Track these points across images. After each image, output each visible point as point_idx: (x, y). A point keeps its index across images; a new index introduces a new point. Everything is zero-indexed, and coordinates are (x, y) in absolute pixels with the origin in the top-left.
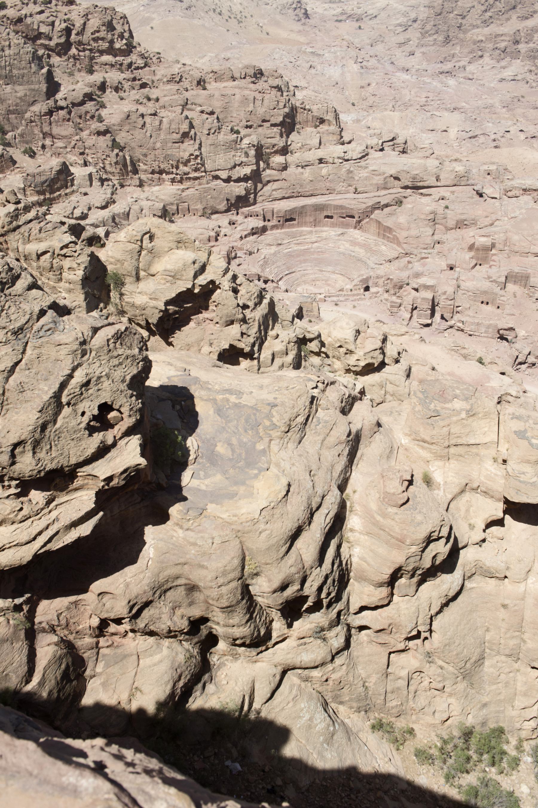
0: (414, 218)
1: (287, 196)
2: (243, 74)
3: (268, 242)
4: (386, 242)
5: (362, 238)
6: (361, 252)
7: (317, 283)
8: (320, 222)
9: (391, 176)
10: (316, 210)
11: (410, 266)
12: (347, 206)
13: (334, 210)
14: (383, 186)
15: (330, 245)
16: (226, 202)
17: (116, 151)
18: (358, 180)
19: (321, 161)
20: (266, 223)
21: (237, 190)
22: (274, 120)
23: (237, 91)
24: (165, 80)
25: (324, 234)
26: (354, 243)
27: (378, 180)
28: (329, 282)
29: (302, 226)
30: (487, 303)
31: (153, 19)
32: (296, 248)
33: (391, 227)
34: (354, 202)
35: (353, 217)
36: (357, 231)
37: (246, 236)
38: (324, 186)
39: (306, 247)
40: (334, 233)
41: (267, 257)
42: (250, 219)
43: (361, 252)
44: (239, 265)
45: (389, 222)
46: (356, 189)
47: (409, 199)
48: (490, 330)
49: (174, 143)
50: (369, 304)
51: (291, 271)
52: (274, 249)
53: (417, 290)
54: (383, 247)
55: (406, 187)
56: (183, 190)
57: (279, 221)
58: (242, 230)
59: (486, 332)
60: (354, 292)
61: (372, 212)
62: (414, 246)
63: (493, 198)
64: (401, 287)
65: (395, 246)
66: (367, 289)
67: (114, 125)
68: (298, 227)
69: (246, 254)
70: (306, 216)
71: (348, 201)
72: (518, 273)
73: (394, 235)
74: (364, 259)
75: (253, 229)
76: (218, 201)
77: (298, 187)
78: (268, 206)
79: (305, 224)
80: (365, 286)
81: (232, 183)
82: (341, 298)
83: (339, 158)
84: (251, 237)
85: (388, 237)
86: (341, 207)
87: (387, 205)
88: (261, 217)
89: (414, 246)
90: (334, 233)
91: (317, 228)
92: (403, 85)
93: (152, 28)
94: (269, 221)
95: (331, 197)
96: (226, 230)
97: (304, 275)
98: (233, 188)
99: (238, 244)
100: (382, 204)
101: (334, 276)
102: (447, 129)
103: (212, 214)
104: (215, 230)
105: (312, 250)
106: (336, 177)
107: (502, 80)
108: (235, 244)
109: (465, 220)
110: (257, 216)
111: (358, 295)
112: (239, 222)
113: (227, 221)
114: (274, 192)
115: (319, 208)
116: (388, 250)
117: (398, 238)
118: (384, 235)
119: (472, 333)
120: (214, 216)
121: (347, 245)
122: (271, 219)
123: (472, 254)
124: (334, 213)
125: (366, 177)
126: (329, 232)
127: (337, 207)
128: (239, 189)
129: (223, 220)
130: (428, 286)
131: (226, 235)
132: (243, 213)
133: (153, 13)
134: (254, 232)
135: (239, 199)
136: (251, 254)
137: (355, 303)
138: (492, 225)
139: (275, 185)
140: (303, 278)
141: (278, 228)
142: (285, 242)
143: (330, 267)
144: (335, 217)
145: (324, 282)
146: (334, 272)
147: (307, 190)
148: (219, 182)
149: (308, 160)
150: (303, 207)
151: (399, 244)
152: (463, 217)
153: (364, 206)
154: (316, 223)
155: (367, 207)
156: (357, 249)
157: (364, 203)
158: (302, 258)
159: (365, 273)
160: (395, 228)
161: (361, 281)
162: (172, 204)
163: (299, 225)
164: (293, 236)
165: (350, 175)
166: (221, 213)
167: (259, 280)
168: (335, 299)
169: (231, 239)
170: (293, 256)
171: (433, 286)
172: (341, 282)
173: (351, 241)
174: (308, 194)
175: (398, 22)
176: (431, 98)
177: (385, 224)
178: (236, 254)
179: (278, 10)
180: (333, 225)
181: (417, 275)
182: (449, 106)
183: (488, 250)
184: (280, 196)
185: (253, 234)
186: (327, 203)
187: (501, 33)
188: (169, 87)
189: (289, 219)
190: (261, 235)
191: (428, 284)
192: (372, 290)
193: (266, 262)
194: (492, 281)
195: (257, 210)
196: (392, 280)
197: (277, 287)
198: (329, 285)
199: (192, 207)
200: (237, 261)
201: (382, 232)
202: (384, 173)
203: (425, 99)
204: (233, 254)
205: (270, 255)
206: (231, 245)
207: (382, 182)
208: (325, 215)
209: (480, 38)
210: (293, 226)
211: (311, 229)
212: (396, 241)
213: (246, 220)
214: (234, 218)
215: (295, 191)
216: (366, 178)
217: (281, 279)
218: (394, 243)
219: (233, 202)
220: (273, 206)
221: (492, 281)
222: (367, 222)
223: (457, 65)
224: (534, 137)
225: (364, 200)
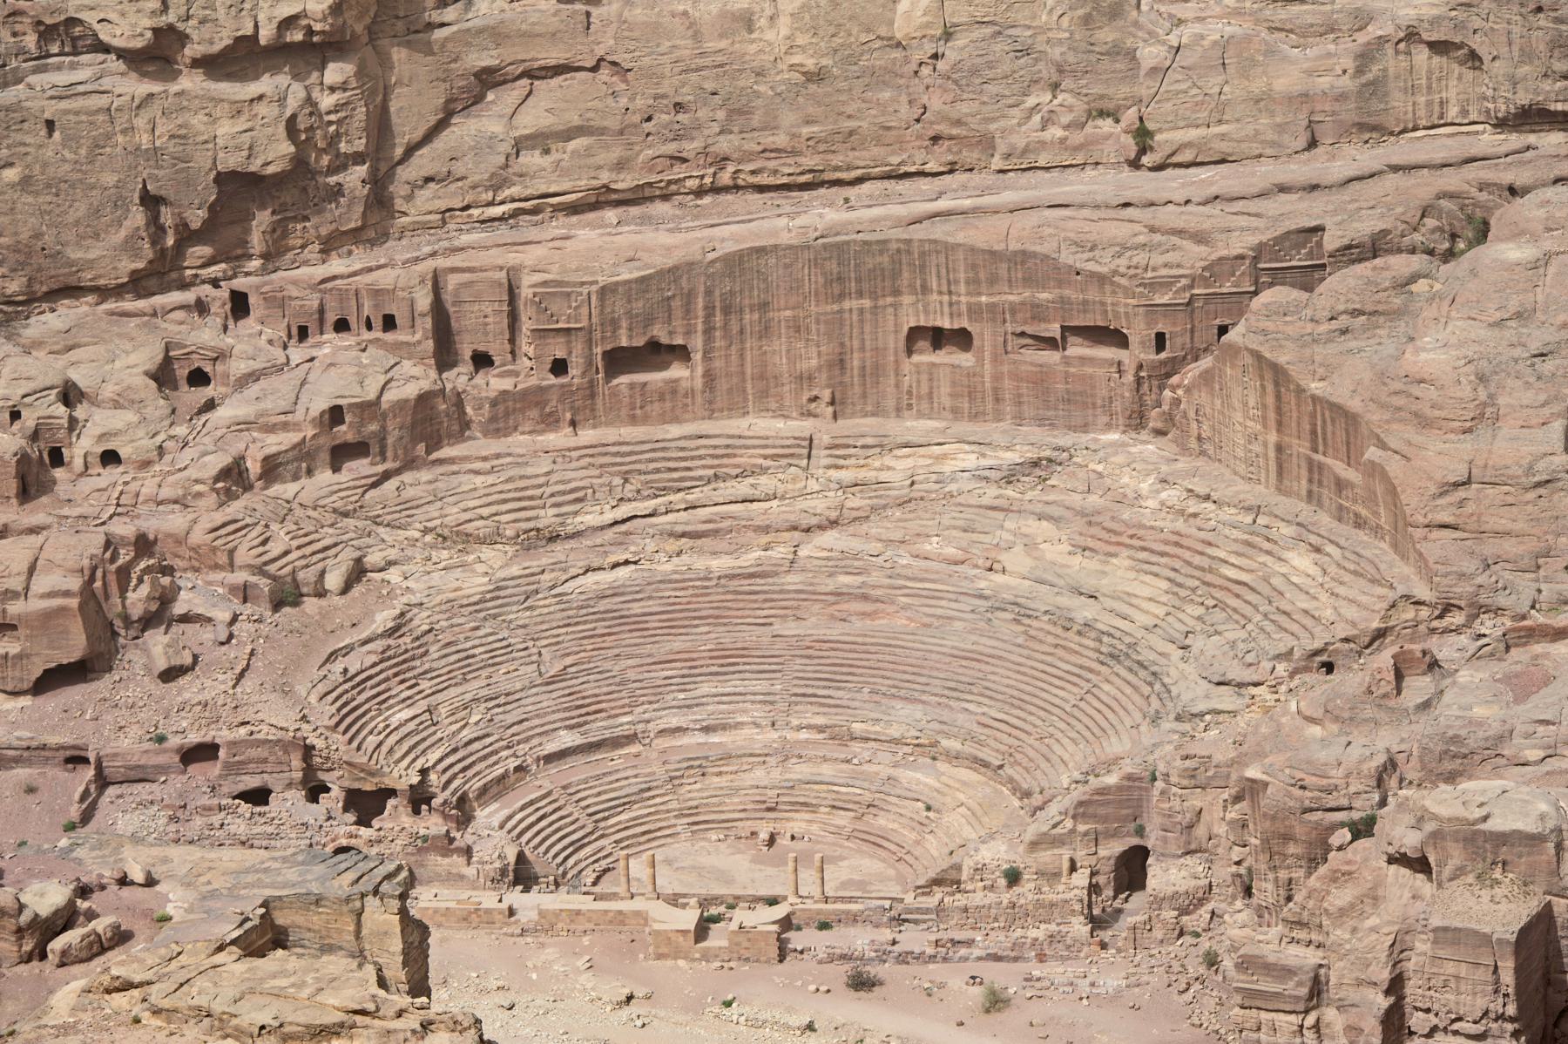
0: (1538, 338)
1: (625, 182)
3: (453, 515)
4: (1325, 520)
5: (1171, 495)
6: (1135, 594)
7: (798, 823)
8: (872, 374)
9: (1412, 36)
10: (837, 287)
11: (1418, 686)
12: (1067, 257)
13: (974, 283)
15: (932, 546)
16: (137, 217)
18: (1160, 72)
20: (459, 377)
21: (225, 129)
25: (897, 469)
26: (1105, 532)
28: (882, 822)
29: (737, 407)
32: (666, 567)
33: (1355, 405)
34: (1118, 231)
35: (1118, 339)
36: (1148, 448)
37: (272, 469)
38: (906, 112)
39: (748, 559)
40: (970, 460)
41: (421, 621)
42: (329, 344)
43: (1135, 594)
44: (170, 674)
45: (1343, 377)
46: (1143, 136)
47: (1528, 209)
50: (1111, 982)
51: (598, 729)
52: (494, 562)
53: (1421, 865)
54: (1301, 561)
55: (1531, 117)
57: (559, 367)
58: (244, 425)
60: (1026, 892)
61: (1238, 303)
62: (1509, 547)
64: (1317, 854)
65: (1379, 550)
66: (1131, 870)
68: (711, 413)
69: (245, 593)
70: (765, 331)
71: (1075, 224)
73: (1374, 470)
74: (1154, 647)
75: (335, 415)
76: (80, 210)
77: (710, 115)
78: (482, 253)
79: (765, 390)
80: (1116, 847)
81: (191, 81)
82: (914, 939)
84: (325, 477)
85: (1341, 485)
86: (1024, 265)
87: (1374, 248)
88: (421, 335)
89: (1509, 547)
90: (970, 460)
94: (482, 361)
95: (956, 194)
96: (122, 418)
97: (699, 766)
98: (198, 121)
99: (200, 522)
100: (1331, 242)
101: (919, 777)
103: (32, 300)
104: (29, 419)
105: (793, 580)
106: (999, 47)
108: (174, 521)
110: (389, 323)
112: (238, 367)
113: (148, 355)
114: (532, 159)
115: (856, 270)
116: (1322, 582)
117: (1393, 491)
120: (50, 321)
121: (1056, 551)
122: (497, 348)
124: (975, 311)
125: (1225, 44)
126: (942, 452)
127: (994, 265)
128: (245, 124)
129: (113, 354)
130: (1502, 839)
131: (110, 458)
132: (278, 302)
134: (344, 438)
135: (239, 189)
136: (286, 596)
137: (1004, 977)
139: (544, 108)
140: (693, 791)
141: (550, 422)
142: (590, 519)
143: (903, 711)
144: (984, 334)
145: (843, 819)
146: (930, 750)
147: (781, 140)
148: (86, 68)
150: (737, 263)
151: (1400, 534)
153: (1194, 256)
155: (1215, 270)
156: (1119, 575)
157: (1200, 238)
158: (705, 638)
159: (1131, 744)
160: (1375, 416)
161: (1082, 810)
163: (719, 395)
164: (669, 475)
165: (1106, 35)
166: (104, 293)
167: (315, 791)
168: (860, 939)
169: (148, 488)
170: (638, 624)
171: (1533, 840)
172: (974, 825)
173: (1089, 517)
174: (786, 170)
177: (1315, 387)
178: (165, 599)
180: (973, 402)
181: (1454, 760)
184: (578, 184)
185: (341, 454)
189: (632, 349)
190: (410, 464)
191: (1496, 824)
192: (1164, 876)
193: (401, 655)
195: (384, 279)
197: (446, 845)
198: (876, 842)
200: (159, 646)
201: (1300, 447)
202: (1362, 19)
204: (138, 598)
205: (452, 606)
206: (124, 529)
207: (1346, 83)
208: (903, 323)
210: (673, 402)
211: (804, 426)
212: (1379, 510)
213: (297, 354)
214: (205, 335)
215: (690, 147)
216: (1222, 56)
217: (496, 788)
218: (1377, 531)
219: (197, 218)
220: (512, 258)
222: (1207, 378)
225: (1195, 218)
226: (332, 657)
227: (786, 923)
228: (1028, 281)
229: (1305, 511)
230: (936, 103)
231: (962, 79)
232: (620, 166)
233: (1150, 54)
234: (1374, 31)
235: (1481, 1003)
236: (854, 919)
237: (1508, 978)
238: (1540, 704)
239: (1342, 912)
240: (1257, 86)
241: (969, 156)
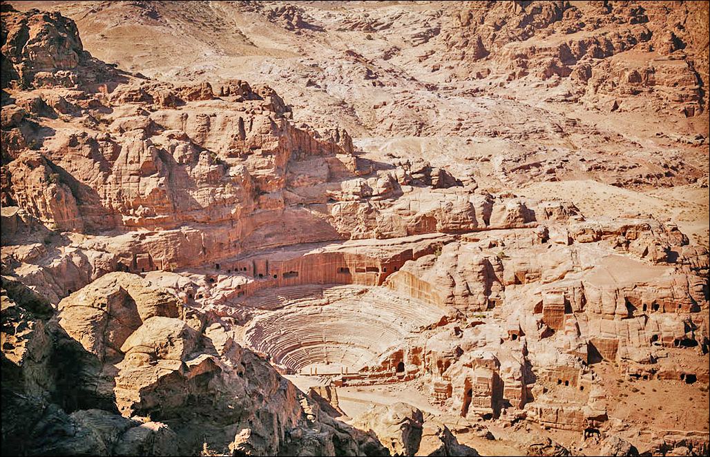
2: (225, 90)
17: (53, 185)
23: (217, 111)
24: (122, 97)
27: (409, 221)
30: (567, 383)
31: (105, 26)
43: (388, 316)
48: (574, 420)
49: (131, 175)
56: (143, 237)
59: (569, 423)
63: (559, 243)
67: (51, 153)
72: (603, 341)
85: (426, 296)
92: (428, 104)
93: (103, 36)
102: (489, 158)
105: (321, 315)
107: (550, 101)
109: (527, 272)
111: (389, 375)
118: (420, 294)
119: (550, 424)
123: (541, 316)
133: (105, 19)
138: (562, 277)
152: (523, 268)
153: (391, 255)
156: (384, 312)
162: (126, 255)
165: (370, 216)
175: (416, 32)
176: (465, 121)
179: (266, 17)
182: (489, 130)
183: (560, 311)
186: (341, 251)
187: (544, 47)
188: (127, 105)
194: (570, 353)
196: (434, 353)
199: (154, 259)
203: (458, 122)
209: (519, 52)
221: (570, 353)
223: (495, 81)
224: (599, 167)
225: (390, 248)
226: (248, 332)
227: (344, 380)
229: (419, 301)
233: (378, 220)
234: (417, 215)
236: (354, 378)
238: (480, 336)
239: (455, 375)
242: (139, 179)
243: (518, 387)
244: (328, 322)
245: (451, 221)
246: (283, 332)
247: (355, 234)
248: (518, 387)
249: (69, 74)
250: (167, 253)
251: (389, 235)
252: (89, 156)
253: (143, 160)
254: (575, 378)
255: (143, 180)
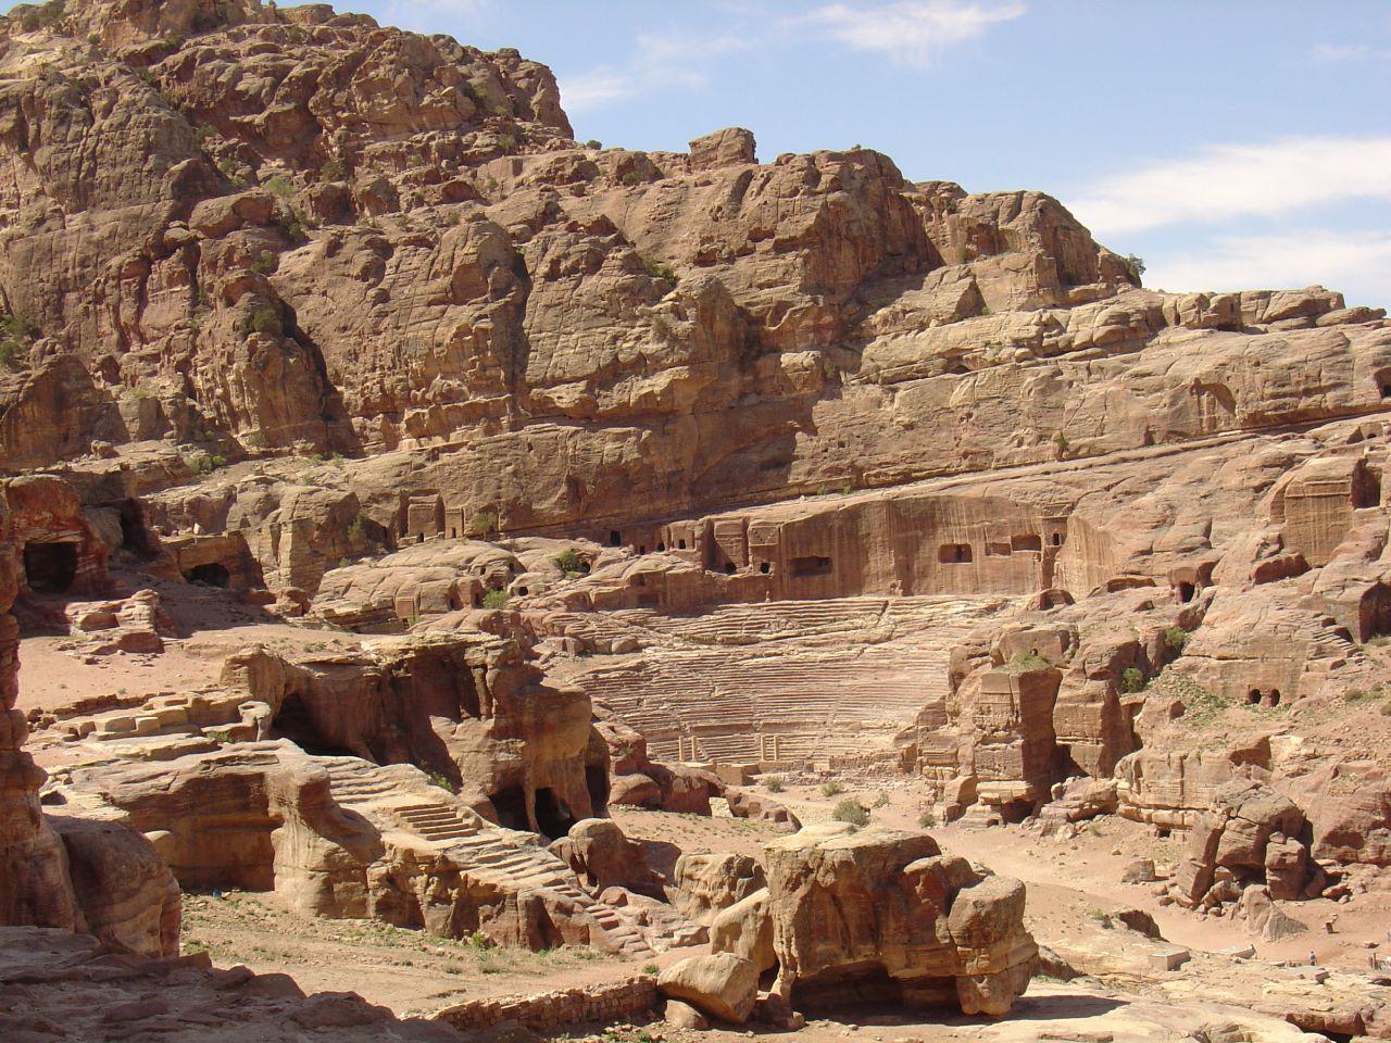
8: (924, 574)
14: (1164, 426)
19: (956, 362)
22: (786, 230)
30: (1275, 697)
32: (794, 658)
40: (962, 608)
46: (1064, 446)
56: (434, 455)
71: (1017, 485)
83: (1017, 343)
91: (917, 598)
106: (1002, 408)
119: (1164, 815)
124: (972, 533)
134: (650, 594)
144: (978, 548)
147: (889, 458)
149: (906, 357)
154: (909, 579)
157: (1079, 485)
162: (388, 497)
164: (810, 621)
165: (1052, 399)
186: (942, 493)
199: (449, 507)
201: (1095, 564)
221: (1307, 605)
228: (994, 513)
230: (965, 436)
231: (985, 424)
232: (809, 473)
233: (1069, 405)
235: (1006, 717)
237: (1017, 701)
240: (1121, 415)
241: (980, 461)
242: (444, 312)
243: (1093, 698)
244: (863, 680)
245: (1269, 391)
246: (717, 694)
247: (1005, 452)
248: (1093, 698)
249: (432, 138)
250: (480, 489)
251: (1091, 447)
252: (364, 276)
253: (457, 263)
254: (1294, 675)
255: (452, 311)
